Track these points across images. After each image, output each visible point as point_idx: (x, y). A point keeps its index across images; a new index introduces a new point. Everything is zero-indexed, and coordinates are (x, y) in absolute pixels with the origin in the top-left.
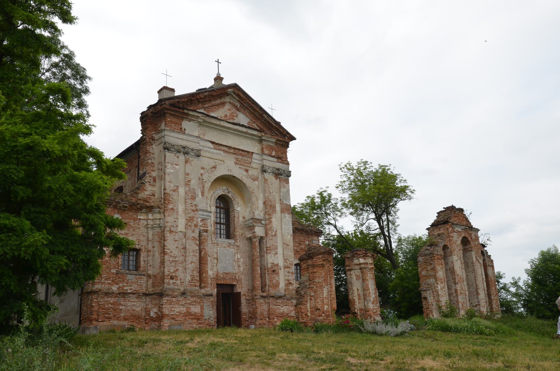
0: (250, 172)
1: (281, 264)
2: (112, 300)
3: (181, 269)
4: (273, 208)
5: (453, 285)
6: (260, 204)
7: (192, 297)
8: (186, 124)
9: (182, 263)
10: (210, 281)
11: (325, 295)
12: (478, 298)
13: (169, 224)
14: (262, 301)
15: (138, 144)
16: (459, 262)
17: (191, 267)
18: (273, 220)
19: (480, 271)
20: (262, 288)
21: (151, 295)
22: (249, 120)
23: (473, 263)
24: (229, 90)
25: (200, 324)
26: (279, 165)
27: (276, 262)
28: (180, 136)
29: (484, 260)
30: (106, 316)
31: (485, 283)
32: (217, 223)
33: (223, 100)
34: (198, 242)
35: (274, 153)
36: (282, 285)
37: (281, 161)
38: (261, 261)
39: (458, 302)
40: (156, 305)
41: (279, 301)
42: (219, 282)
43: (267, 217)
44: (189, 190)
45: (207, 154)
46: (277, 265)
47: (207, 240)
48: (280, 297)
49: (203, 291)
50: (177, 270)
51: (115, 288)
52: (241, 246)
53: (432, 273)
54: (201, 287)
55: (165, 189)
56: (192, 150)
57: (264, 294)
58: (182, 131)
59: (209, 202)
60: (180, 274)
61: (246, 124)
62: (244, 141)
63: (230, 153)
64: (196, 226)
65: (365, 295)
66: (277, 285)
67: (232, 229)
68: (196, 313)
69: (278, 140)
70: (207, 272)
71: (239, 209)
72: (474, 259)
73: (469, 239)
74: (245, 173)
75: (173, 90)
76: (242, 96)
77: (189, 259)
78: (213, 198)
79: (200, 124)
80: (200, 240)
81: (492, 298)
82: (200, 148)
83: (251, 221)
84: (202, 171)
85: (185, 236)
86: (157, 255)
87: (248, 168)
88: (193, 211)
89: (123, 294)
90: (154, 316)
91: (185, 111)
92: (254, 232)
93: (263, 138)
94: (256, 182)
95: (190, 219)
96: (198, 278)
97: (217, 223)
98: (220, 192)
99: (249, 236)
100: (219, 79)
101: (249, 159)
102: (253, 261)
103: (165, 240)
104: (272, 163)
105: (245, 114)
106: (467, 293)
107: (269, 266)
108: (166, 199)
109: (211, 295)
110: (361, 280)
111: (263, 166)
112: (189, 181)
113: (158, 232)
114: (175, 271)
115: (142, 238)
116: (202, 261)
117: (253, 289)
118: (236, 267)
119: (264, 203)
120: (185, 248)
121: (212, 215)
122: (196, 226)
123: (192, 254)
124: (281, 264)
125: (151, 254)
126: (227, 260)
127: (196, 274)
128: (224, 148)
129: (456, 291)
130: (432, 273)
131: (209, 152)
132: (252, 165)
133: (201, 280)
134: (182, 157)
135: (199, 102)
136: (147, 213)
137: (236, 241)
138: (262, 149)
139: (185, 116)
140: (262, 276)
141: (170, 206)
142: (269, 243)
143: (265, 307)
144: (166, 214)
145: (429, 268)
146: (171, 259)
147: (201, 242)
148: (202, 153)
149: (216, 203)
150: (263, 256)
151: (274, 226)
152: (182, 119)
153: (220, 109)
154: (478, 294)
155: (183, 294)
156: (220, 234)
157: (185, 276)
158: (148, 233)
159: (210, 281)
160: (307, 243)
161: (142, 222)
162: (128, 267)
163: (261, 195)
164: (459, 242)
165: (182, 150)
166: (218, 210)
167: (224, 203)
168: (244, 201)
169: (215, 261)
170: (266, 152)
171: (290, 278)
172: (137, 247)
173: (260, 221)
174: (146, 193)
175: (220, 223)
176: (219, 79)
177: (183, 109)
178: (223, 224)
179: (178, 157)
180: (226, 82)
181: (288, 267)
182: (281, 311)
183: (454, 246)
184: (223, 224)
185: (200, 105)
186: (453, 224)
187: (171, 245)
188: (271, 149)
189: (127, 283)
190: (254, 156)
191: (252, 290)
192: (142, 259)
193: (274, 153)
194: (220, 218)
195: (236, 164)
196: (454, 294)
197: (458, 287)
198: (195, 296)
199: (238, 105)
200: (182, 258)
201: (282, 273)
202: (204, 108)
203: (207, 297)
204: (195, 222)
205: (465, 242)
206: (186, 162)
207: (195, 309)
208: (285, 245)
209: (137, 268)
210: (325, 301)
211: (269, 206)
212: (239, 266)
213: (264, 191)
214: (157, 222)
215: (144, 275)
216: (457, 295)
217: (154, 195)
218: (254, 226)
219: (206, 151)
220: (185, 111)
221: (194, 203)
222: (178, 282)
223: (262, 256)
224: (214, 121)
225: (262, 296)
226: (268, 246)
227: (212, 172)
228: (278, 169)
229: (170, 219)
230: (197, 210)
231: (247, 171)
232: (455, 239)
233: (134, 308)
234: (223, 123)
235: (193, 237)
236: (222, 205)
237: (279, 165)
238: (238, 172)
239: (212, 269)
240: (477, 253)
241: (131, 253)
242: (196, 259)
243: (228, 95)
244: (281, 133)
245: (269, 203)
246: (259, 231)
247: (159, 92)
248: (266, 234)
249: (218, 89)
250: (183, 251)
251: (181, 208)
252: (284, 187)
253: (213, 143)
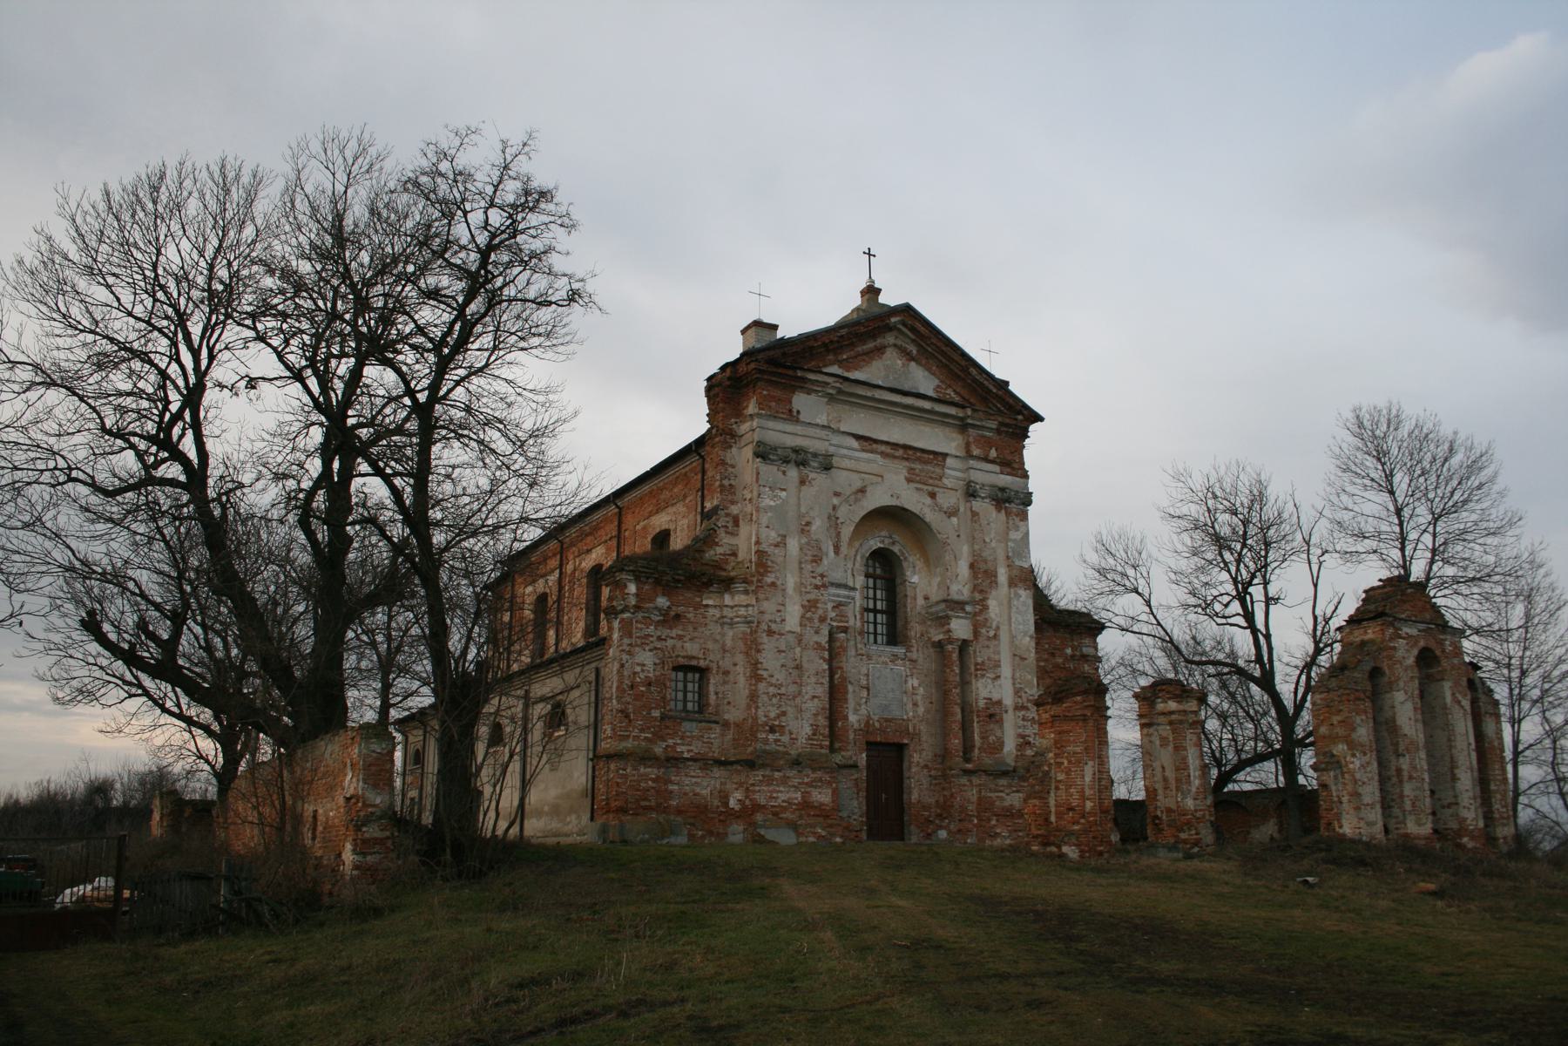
0: (940, 499)
1: (1009, 701)
2: (652, 772)
3: (790, 710)
4: (991, 576)
5: (1393, 758)
6: (963, 569)
7: (814, 770)
8: (800, 401)
9: (794, 698)
10: (852, 736)
11: (1088, 779)
12: (1453, 788)
13: (767, 617)
14: (964, 780)
15: (700, 442)
16: (1409, 706)
17: (812, 706)
18: (992, 603)
19: (1463, 726)
20: (965, 753)
21: (732, 763)
22: (937, 382)
23: (1445, 707)
24: (893, 320)
25: (831, 826)
26: (1005, 480)
27: (996, 697)
28: (789, 428)
29: (1474, 702)
30: (643, 803)
31: (1474, 755)
32: (867, 610)
34: (826, 655)
35: (993, 453)
36: (1010, 746)
38: (963, 692)
39: (1402, 796)
40: (741, 784)
41: (1003, 782)
42: (872, 739)
43: (978, 596)
44: (808, 544)
45: (846, 463)
46: (999, 703)
47: (845, 650)
48: (1005, 774)
49: (838, 758)
50: (784, 714)
51: (658, 750)
52: (920, 661)
53: (1340, 731)
54: (832, 749)
55: (758, 543)
56: (815, 455)
57: (969, 766)
58: (792, 417)
59: (850, 565)
60: (791, 723)
61: (931, 393)
62: (927, 429)
63: (895, 457)
64: (822, 620)
65: (1178, 780)
66: (1000, 744)
67: (900, 624)
68: (822, 804)
69: (1001, 424)
70: (846, 718)
71: (915, 579)
72: (1449, 699)
73: (1438, 653)
74: (928, 501)
75: (775, 327)
76: (922, 329)
77: (809, 690)
79: (832, 399)
80: (831, 650)
81: (1493, 787)
82: (832, 450)
83: (943, 606)
84: (835, 501)
85: (800, 641)
86: (742, 680)
88: (817, 587)
89: (673, 761)
90: (737, 808)
91: (799, 373)
92: (949, 631)
94: (954, 520)
95: (811, 606)
96: (827, 731)
97: (867, 610)
98: (875, 544)
99: (937, 638)
100: (871, 292)
101: (938, 470)
102: (945, 694)
103: (759, 651)
104: (989, 476)
105: (929, 370)
106: (1426, 776)
107: (982, 703)
108: (763, 562)
109: (855, 766)
110: (1170, 748)
111: (969, 484)
112: (808, 524)
113: (744, 633)
114: (778, 717)
115: (710, 645)
116: (836, 693)
117: (944, 755)
118: (910, 706)
119: (972, 566)
120: (798, 667)
121: (857, 595)
122: (822, 620)
123: (813, 680)
124: (1009, 701)
125: (731, 677)
126: (891, 687)
127: (823, 721)
128: (883, 448)
129: (1399, 770)
130: (1340, 731)
131: (850, 458)
132: (945, 481)
133: (833, 734)
134: (793, 473)
135: (828, 351)
136: (721, 593)
137: (909, 649)
138: (968, 445)
140: (966, 727)
141: (769, 580)
142: (979, 654)
143: (972, 795)
144: (761, 596)
145: (1335, 719)
146: (772, 690)
147: (833, 653)
148: (835, 461)
149: (867, 565)
150: (969, 683)
151: (992, 615)
152: (793, 389)
154: (1454, 778)
155: (796, 763)
156: (875, 634)
157: (802, 728)
158: (723, 635)
159: (852, 736)
160: (1069, 651)
161: (712, 611)
162: (685, 706)
163: (965, 549)
164: (1411, 661)
165: (793, 456)
166: (871, 581)
167: (885, 567)
168: (927, 562)
169: (865, 693)
170: (976, 452)
171: (1027, 732)
172: (702, 664)
173: (958, 605)
174: (719, 550)
175: (875, 611)
176: (871, 292)
178: (881, 612)
179: (784, 473)
180: (889, 298)
181: (1023, 708)
182: (1006, 804)
183: (1399, 670)
184: (881, 612)
185: (831, 357)
186: (1396, 619)
187: (770, 661)
188: (989, 443)
189: (682, 738)
190: (949, 461)
191: (944, 757)
192: (712, 689)
193: (993, 453)
194: (875, 599)
195: (909, 480)
196: (1394, 780)
197: (1404, 763)
198: (820, 769)
199: (914, 350)
200: (792, 689)
201: (1010, 720)
202: (841, 363)
203: (845, 771)
204: (820, 612)
205: (1426, 659)
206: (802, 482)
207: (822, 796)
208: (1018, 658)
209: (702, 705)
210: (1088, 792)
211: (982, 574)
212: (915, 705)
213: (972, 540)
214: (742, 611)
215: (716, 722)
216: (1401, 782)
217: (734, 554)
218: (948, 617)
219: (844, 456)
220: (799, 373)
221: (819, 570)
222: (785, 739)
223: (965, 683)
224: (861, 391)
225: (967, 772)
226: (979, 660)
227: (856, 500)
228: (1003, 490)
229: (769, 606)
230: (824, 586)
231: (933, 495)
232: (1400, 654)
233: (698, 790)
234: (878, 394)
236: (878, 571)
237: (1005, 480)
238: (912, 499)
239: (856, 711)
240: (1456, 684)
241: (690, 676)
242: (822, 691)
243: (890, 329)
244: (1010, 407)
245: (983, 567)
246: (960, 628)
247: (743, 332)
248: (976, 633)
249: (868, 320)
250: (795, 673)
251: (791, 581)
252: (1017, 528)
253: (858, 437)
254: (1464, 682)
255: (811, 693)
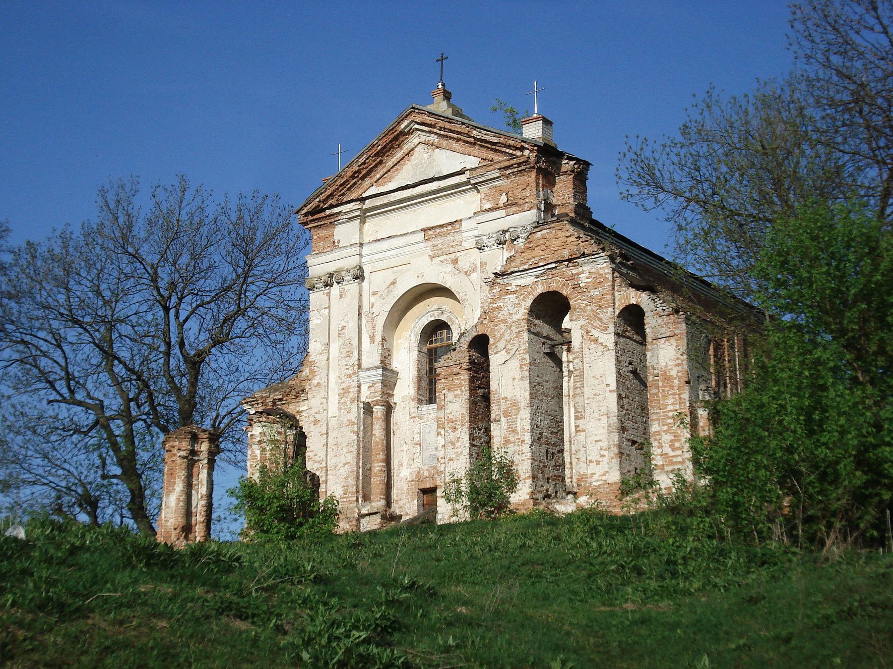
13: (313, 411)
16: (515, 364)
24: (402, 126)
33: (406, 148)
37: (514, 208)
56: (348, 271)
58: (334, 245)
74: (450, 267)
78: (413, 337)
84: (373, 299)
87: (458, 254)
91: (328, 212)
93: (472, 182)
123: (345, 450)
139: (332, 221)
153: (405, 167)
177: (324, 210)
179: (329, 294)
185: (368, 181)
199: (434, 138)
219: (379, 260)
235: (349, 420)
243: (411, 132)
254: (609, 315)
255: (343, 462)
